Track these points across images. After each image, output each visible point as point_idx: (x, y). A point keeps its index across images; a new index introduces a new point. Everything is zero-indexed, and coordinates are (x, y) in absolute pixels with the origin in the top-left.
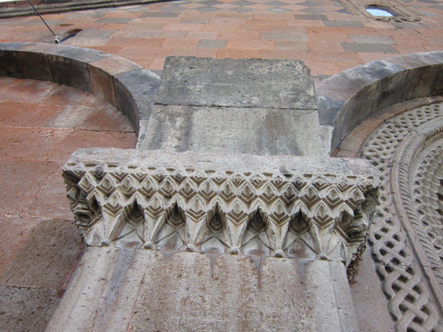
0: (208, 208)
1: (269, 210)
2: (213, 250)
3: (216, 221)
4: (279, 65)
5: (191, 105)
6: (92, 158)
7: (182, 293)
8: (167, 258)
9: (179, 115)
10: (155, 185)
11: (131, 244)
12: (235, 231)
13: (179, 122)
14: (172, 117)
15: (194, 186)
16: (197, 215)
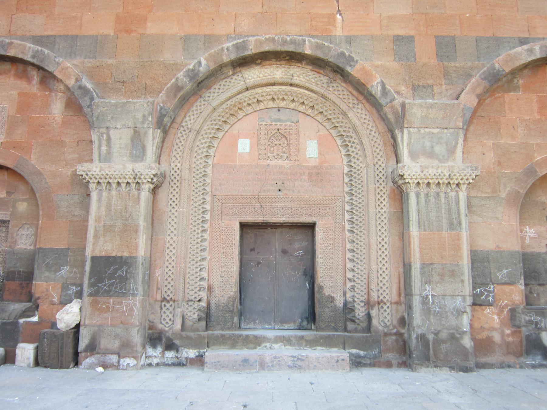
0: (116, 181)
1: (130, 181)
2: (119, 190)
3: (119, 184)
4: (138, 104)
5: (107, 128)
6: (83, 168)
7: (113, 202)
8: (109, 193)
9: (104, 133)
10: (102, 177)
11: (101, 190)
12: (124, 186)
13: (105, 136)
14: (102, 134)
15: (111, 176)
16: (114, 183)
